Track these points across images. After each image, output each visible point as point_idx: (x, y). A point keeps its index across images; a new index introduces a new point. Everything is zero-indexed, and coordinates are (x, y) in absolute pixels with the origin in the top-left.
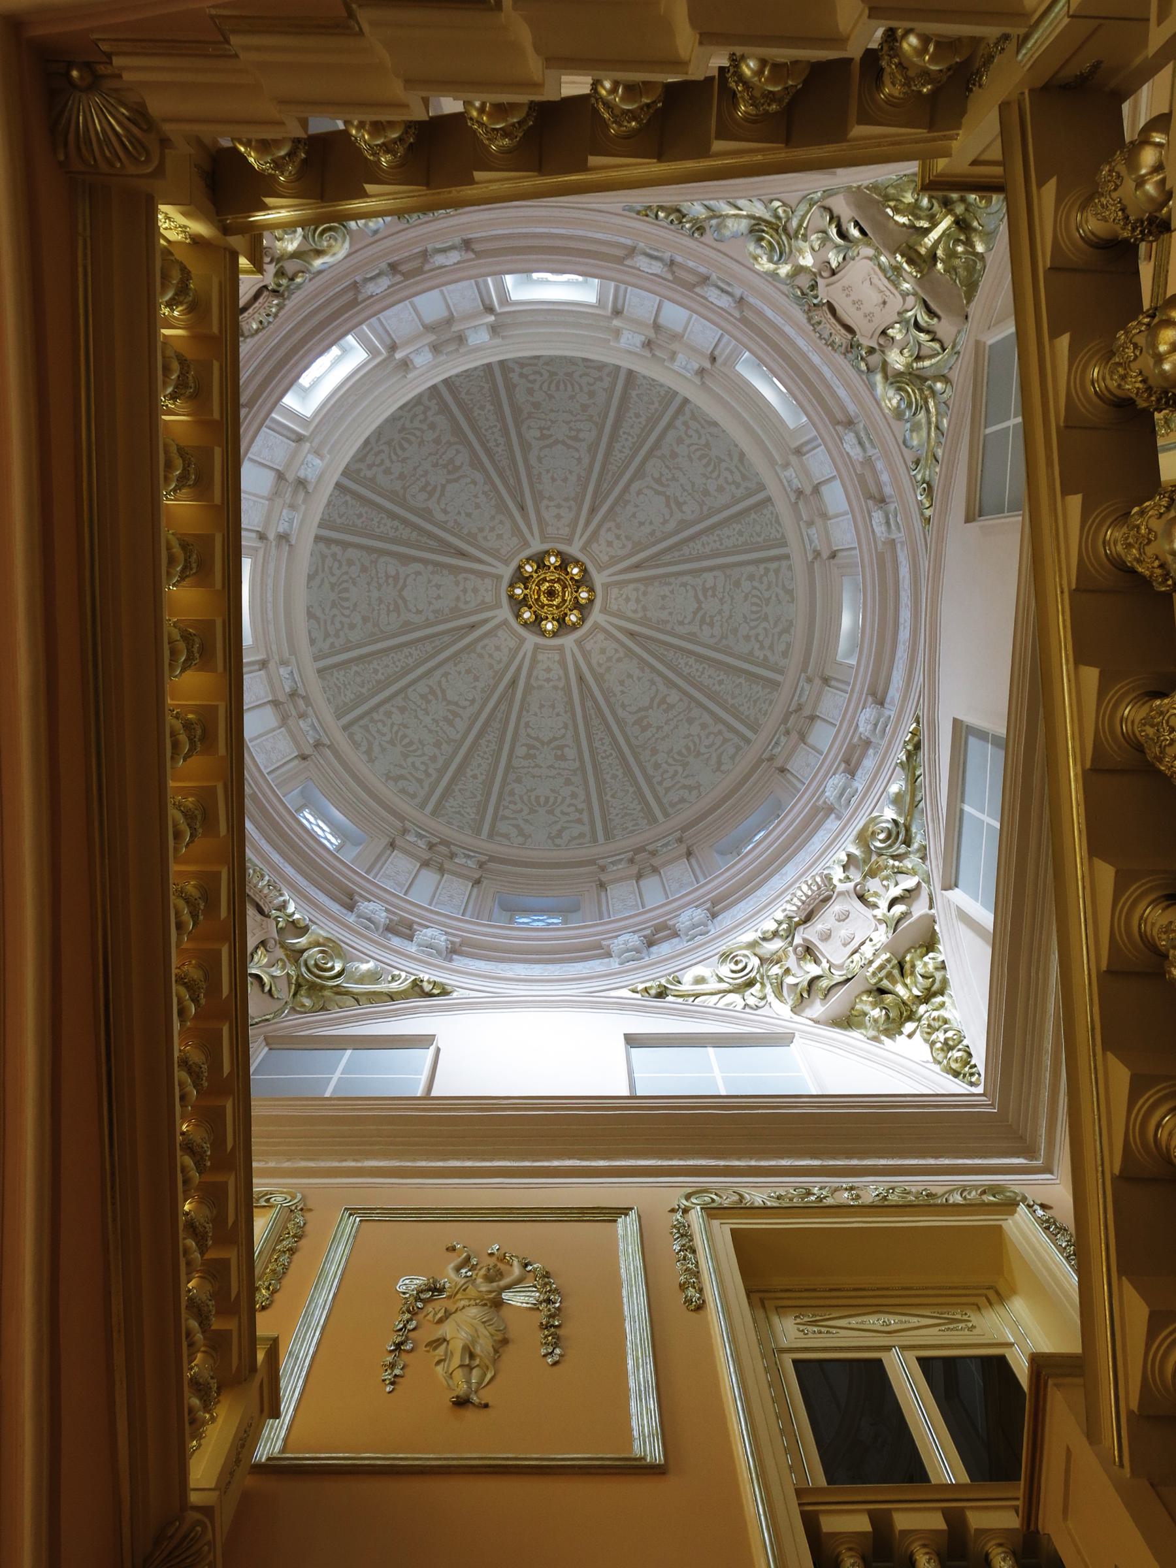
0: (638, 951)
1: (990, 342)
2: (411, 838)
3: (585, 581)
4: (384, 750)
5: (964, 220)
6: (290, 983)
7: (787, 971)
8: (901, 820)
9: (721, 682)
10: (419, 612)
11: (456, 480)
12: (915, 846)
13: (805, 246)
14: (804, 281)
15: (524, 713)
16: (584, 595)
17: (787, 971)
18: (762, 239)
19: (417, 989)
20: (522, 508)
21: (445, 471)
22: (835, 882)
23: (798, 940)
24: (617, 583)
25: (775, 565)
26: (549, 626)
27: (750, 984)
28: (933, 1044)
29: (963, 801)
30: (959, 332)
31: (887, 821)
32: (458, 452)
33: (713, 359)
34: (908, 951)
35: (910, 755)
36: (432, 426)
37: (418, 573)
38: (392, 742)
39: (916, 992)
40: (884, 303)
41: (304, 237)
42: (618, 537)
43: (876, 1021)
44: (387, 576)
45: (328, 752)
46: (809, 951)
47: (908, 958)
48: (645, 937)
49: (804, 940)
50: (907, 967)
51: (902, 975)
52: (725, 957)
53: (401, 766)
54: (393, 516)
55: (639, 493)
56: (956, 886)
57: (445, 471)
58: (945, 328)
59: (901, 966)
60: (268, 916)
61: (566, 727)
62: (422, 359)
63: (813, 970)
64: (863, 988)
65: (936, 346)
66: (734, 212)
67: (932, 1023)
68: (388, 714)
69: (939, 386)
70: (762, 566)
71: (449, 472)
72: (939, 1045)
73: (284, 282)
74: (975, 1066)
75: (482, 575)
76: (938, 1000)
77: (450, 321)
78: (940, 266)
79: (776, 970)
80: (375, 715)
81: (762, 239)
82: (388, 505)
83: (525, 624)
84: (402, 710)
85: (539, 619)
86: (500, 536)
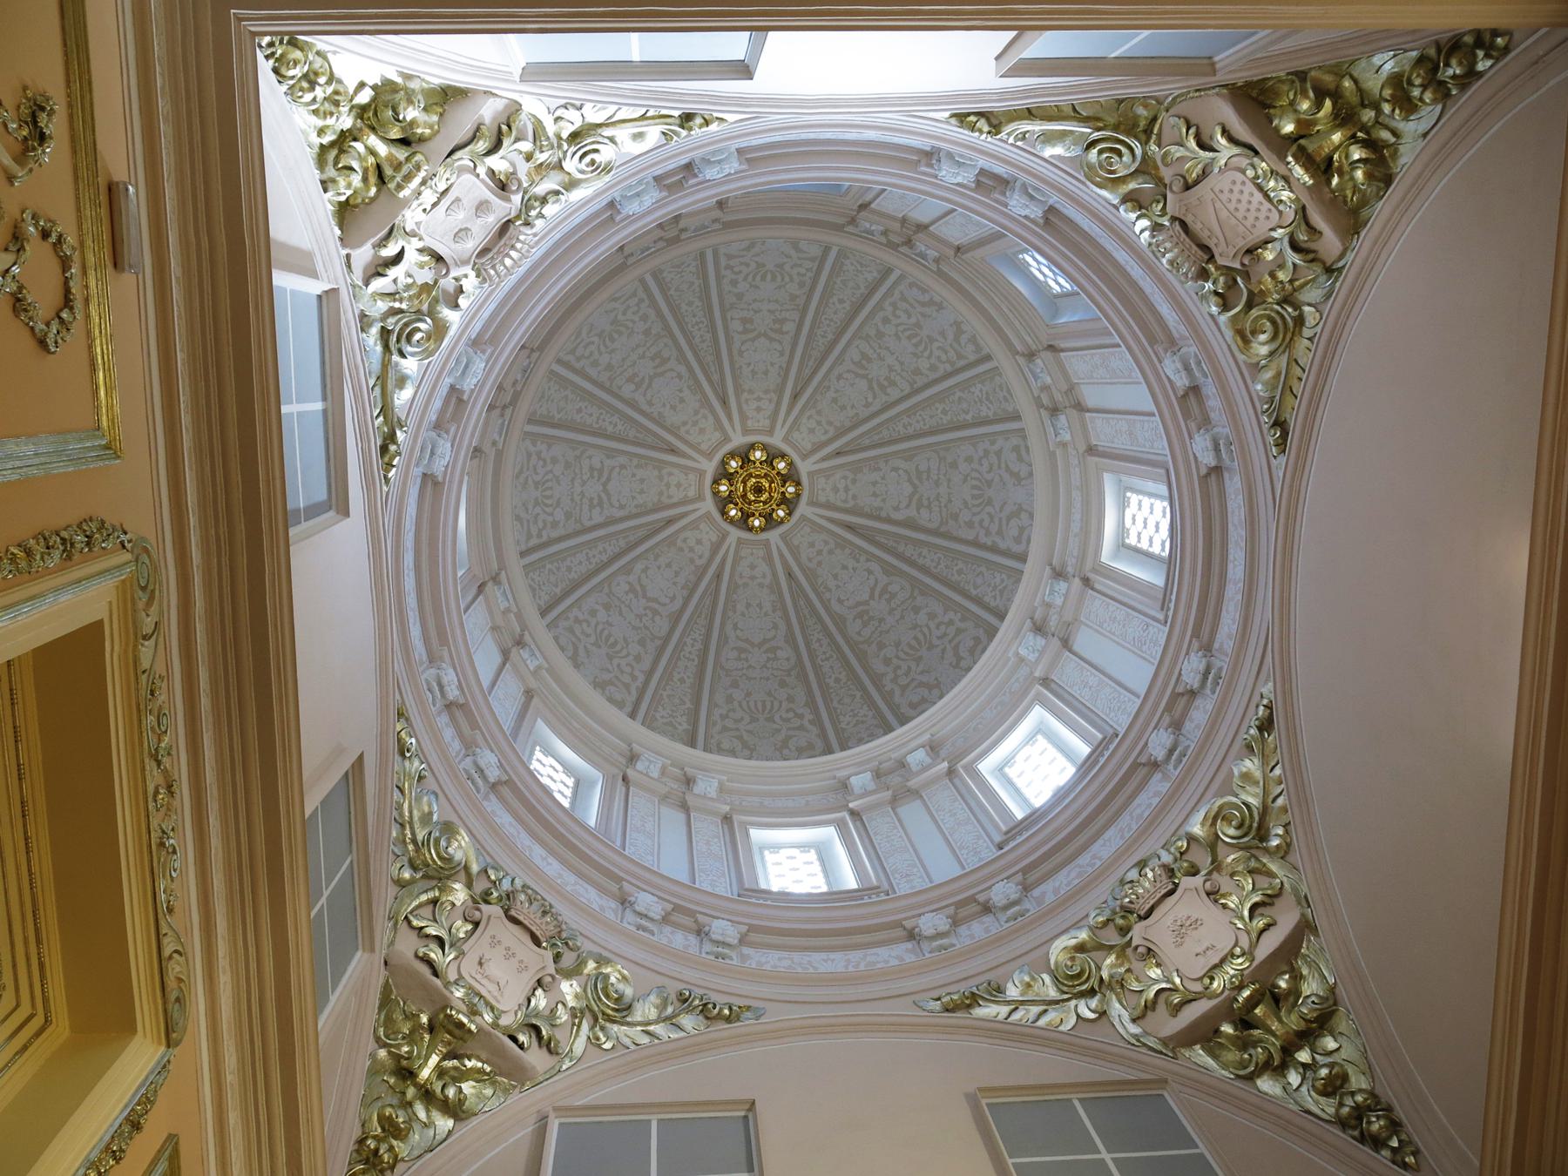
0: (708, 162)
1: (359, 954)
2: (932, 254)
3: (723, 503)
4: (943, 333)
5: (404, 1079)
6: (1159, 135)
7: (529, 157)
8: (396, 358)
10: (895, 469)
11: (859, 604)
12: (375, 330)
13: (571, 1003)
14: (568, 959)
16: (723, 488)
17: (529, 157)
18: (617, 1001)
19: (995, 122)
22: (472, 274)
23: (517, 199)
24: (692, 501)
26: (758, 454)
27: (575, 136)
28: (331, 79)
29: (325, 411)
30: (392, 943)
31: (413, 354)
32: (859, 633)
33: (625, 779)
34: (373, 200)
35: (391, 438)
36: (887, 661)
37: (896, 509)
38: (931, 340)
39: (359, 146)
40: (481, 964)
41: (1099, 968)
42: (691, 550)
43: (410, 102)
44: (929, 507)
46: (502, 186)
47: (373, 190)
48: (695, 176)
49: (508, 200)
50: (373, 179)
51: (379, 167)
52: (607, 169)
53: (923, 315)
56: (319, 297)
58: (407, 945)
59: (381, 179)
60: (1173, 219)
61: (741, 353)
62: (918, 758)
63: (497, 163)
64: (431, 145)
65: (415, 923)
66: (651, 1028)
67: (333, 109)
68: (933, 368)
69: (407, 875)
70: (545, 538)
71: (867, 612)
72: (322, 80)
73: (1120, 922)
74: (267, 57)
75: (828, 506)
76: (328, 138)
77: (894, 802)
78: (424, 1019)
79: (541, 157)
80: (949, 368)
81: (617, 1001)
82: (928, 580)
83: (783, 456)
84: (917, 372)
85: (770, 462)
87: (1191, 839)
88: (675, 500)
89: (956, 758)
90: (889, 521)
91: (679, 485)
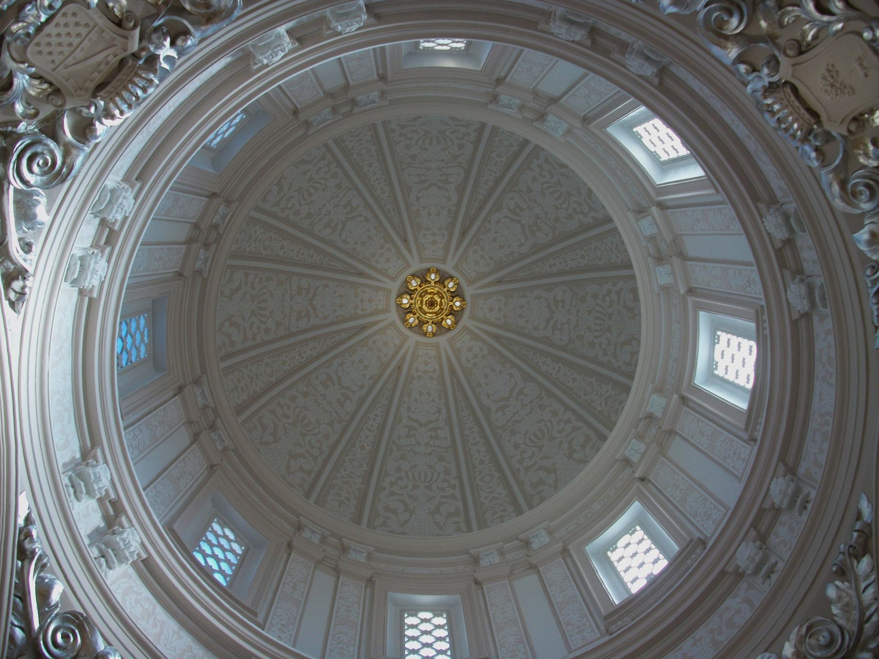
9: (362, 448)
16: (430, 329)
20: (499, 282)
21: (531, 224)
25: (459, 496)
32: (547, 235)
37: (449, 199)
42: (475, 356)
45: (301, 132)
54: (497, 182)
57: (531, 224)
75: (447, 248)
83: (407, 282)
87: (740, 59)
88: (437, 366)
89: (648, 199)
90: (458, 205)
91: (426, 363)
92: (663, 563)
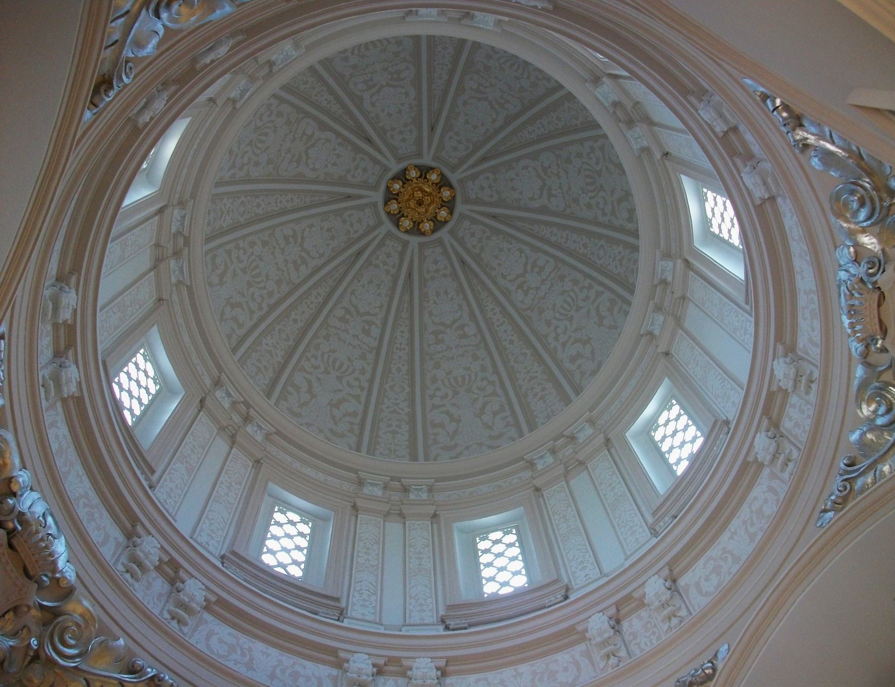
6: (26, 654)
15: (356, 281)
21: (390, 77)
32: (407, 68)
38: (244, 271)
44: (304, 134)
54: (331, 91)
55: (526, 167)
57: (390, 77)
61: (381, 307)
82: (330, 81)
86: (404, 140)
92: (521, 581)
